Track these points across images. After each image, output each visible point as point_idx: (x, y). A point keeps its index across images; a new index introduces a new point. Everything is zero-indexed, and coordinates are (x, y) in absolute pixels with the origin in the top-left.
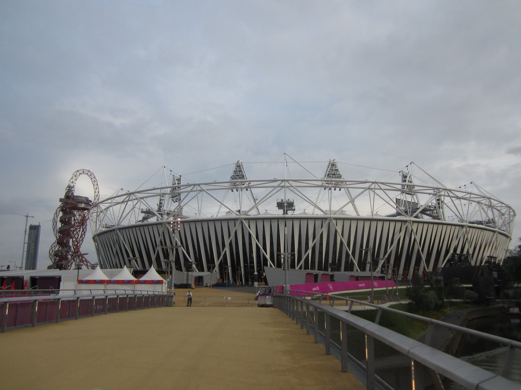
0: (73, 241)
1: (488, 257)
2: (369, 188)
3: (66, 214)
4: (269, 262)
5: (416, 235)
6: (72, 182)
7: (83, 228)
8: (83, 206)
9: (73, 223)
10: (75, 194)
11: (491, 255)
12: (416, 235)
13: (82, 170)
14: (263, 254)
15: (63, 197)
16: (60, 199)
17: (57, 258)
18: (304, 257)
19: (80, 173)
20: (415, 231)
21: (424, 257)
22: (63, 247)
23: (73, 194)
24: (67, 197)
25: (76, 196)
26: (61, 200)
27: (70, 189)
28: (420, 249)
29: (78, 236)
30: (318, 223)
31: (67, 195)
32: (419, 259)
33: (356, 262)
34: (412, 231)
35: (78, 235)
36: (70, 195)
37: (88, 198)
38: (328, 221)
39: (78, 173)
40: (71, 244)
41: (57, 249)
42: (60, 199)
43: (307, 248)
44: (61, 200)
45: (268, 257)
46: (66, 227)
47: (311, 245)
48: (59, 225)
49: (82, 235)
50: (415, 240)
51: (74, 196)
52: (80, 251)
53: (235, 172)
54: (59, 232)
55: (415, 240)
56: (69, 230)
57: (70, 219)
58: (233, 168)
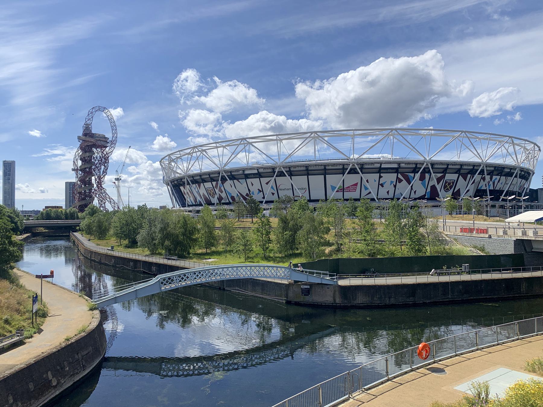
0: (96, 179)
3: (86, 152)
8: (99, 143)
9: (93, 161)
10: (93, 132)
15: (81, 134)
16: (78, 136)
19: (97, 110)
23: (91, 131)
24: (85, 135)
31: (85, 133)
35: (100, 172)
37: (105, 136)
40: (93, 181)
42: (78, 136)
44: (79, 138)
48: (80, 163)
49: (104, 172)
54: (81, 170)
56: (90, 168)
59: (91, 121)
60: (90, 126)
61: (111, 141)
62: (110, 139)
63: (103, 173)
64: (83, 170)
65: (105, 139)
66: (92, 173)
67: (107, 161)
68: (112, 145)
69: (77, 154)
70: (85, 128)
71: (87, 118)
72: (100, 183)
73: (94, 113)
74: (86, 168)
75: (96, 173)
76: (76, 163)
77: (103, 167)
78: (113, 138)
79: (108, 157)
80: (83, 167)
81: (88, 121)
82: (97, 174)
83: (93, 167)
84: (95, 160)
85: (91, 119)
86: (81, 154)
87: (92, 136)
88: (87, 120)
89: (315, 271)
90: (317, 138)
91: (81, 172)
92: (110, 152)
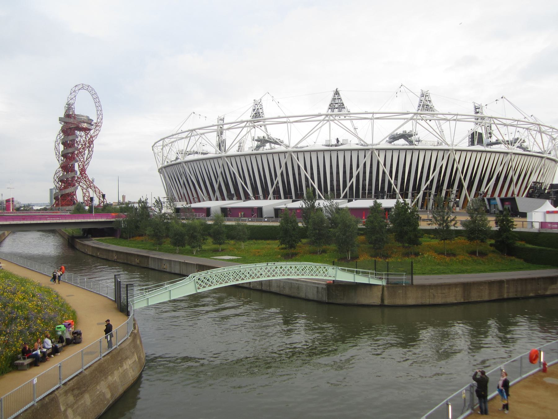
0: (79, 166)
1: (534, 182)
2: (411, 119)
4: (317, 191)
5: (459, 164)
6: (72, 98)
7: (89, 150)
8: (85, 125)
9: (76, 145)
10: (76, 113)
11: (538, 181)
12: (459, 164)
13: (81, 85)
14: (311, 184)
15: (62, 116)
16: (59, 118)
17: (63, 184)
18: (349, 185)
20: (457, 160)
21: (466, 185)
22: (67, 172)
23: (74, 112)
24: (68, 116)
25: (77, 115)
26: (61, 119)
27: (69, 107)
28: (462, 178)
29: (84, 159)
30: (441, 154)
32: (460, 186)
33: (398, 191)
34: (454, 160)
35: (84, 158)
36: (71, 113)
37: (89, 117)
38: (449, 152)
39: (77, 89)
40: (76, 168)
41: (61, 175)
42: (59, 118)
43: (351, 177)
44: (61, 119)
45: (316, 186)
46: (70, 150)
47: (355, 174)
48: (62, 148)
50: (457, 169)
51: (75, 114)
52: (87, 176)
53: (334, 99)
54: (62, 156)
55: (457, 169)
56: (73, 153)
57: (73, 141)
58: (331, 96)
59: (74, 101)
60: (73, 107)
61: (96, 123)
62: (95, 121)
63: (87, 160)
64: (64, 155)
65: (89, 122)
66: (74, 158)
67: (92, 146)
68: (97, 128)
69: (58, 137)
70: (67, 108)
71: (69, 97)
72: (83, 171)
73: (77, 92)
74: (68, 153)
75: (79, 159)
76: (58, 148)
77: (87, 152)
78: (98, 120)
79: (93, 141)
80: (66, 152)
81: (71, 101)
82: (80, 160)
83: (76, 152)
84: (78, 145)
85: (74, 98)
86: (63, 137)
87: (74, 117)
88: (69, 100)
89: (361, 270)
90: (332, 120)
91: (63, 158)
92: (95, 136)
